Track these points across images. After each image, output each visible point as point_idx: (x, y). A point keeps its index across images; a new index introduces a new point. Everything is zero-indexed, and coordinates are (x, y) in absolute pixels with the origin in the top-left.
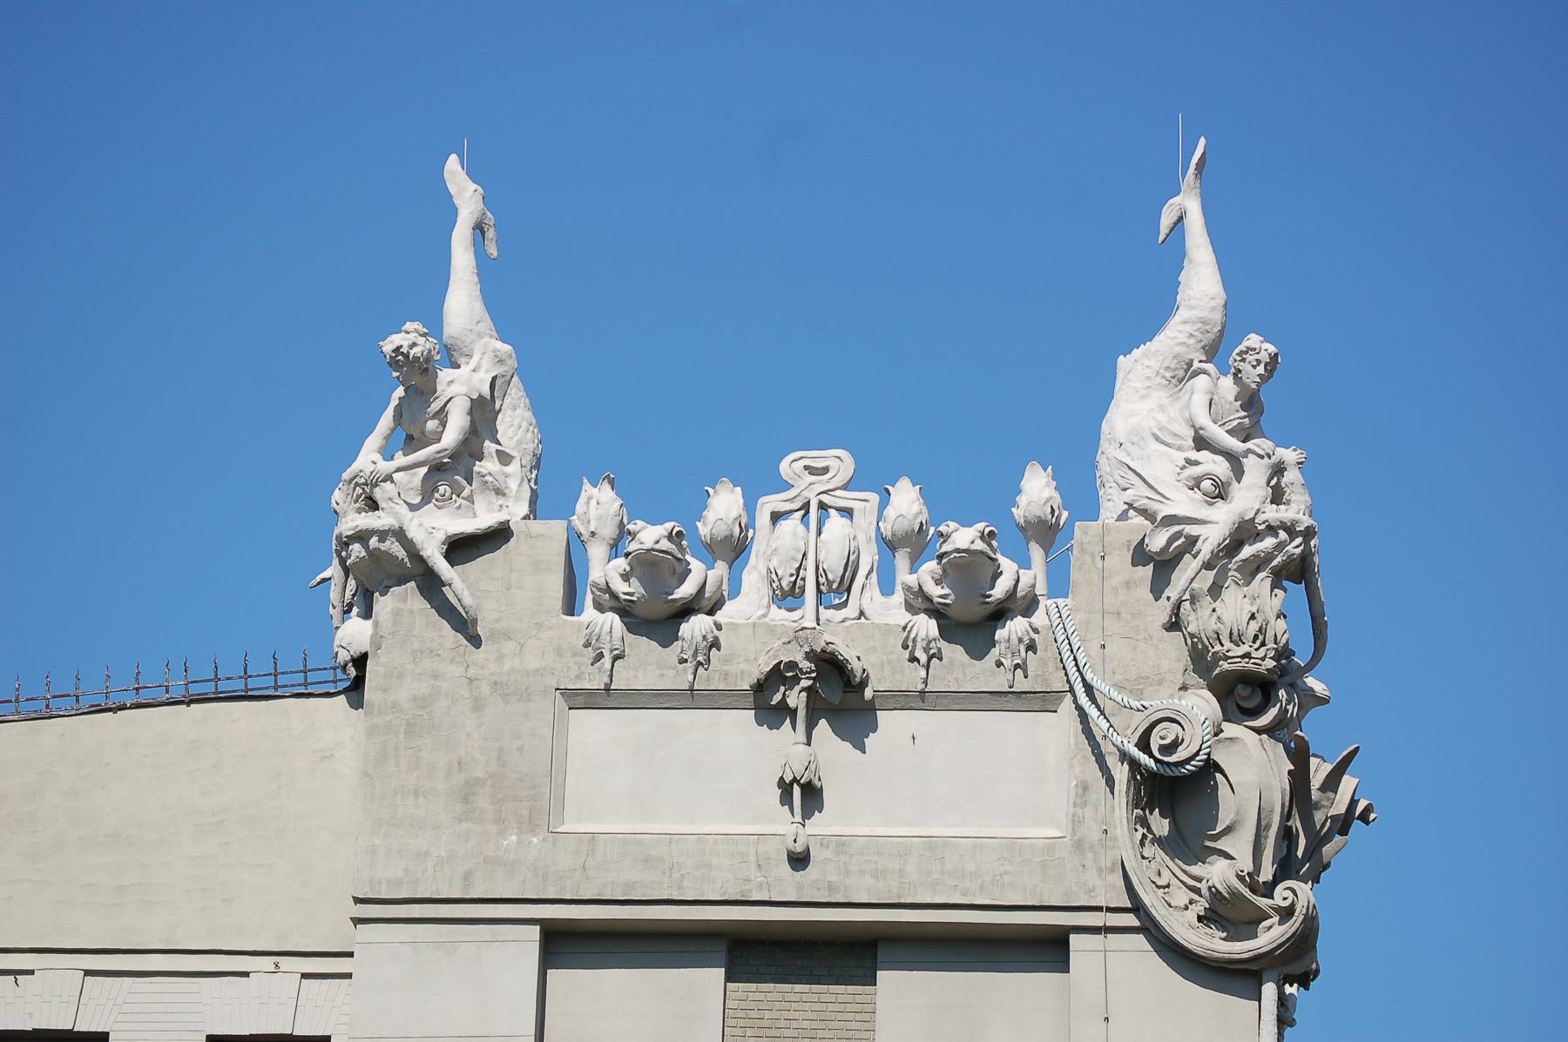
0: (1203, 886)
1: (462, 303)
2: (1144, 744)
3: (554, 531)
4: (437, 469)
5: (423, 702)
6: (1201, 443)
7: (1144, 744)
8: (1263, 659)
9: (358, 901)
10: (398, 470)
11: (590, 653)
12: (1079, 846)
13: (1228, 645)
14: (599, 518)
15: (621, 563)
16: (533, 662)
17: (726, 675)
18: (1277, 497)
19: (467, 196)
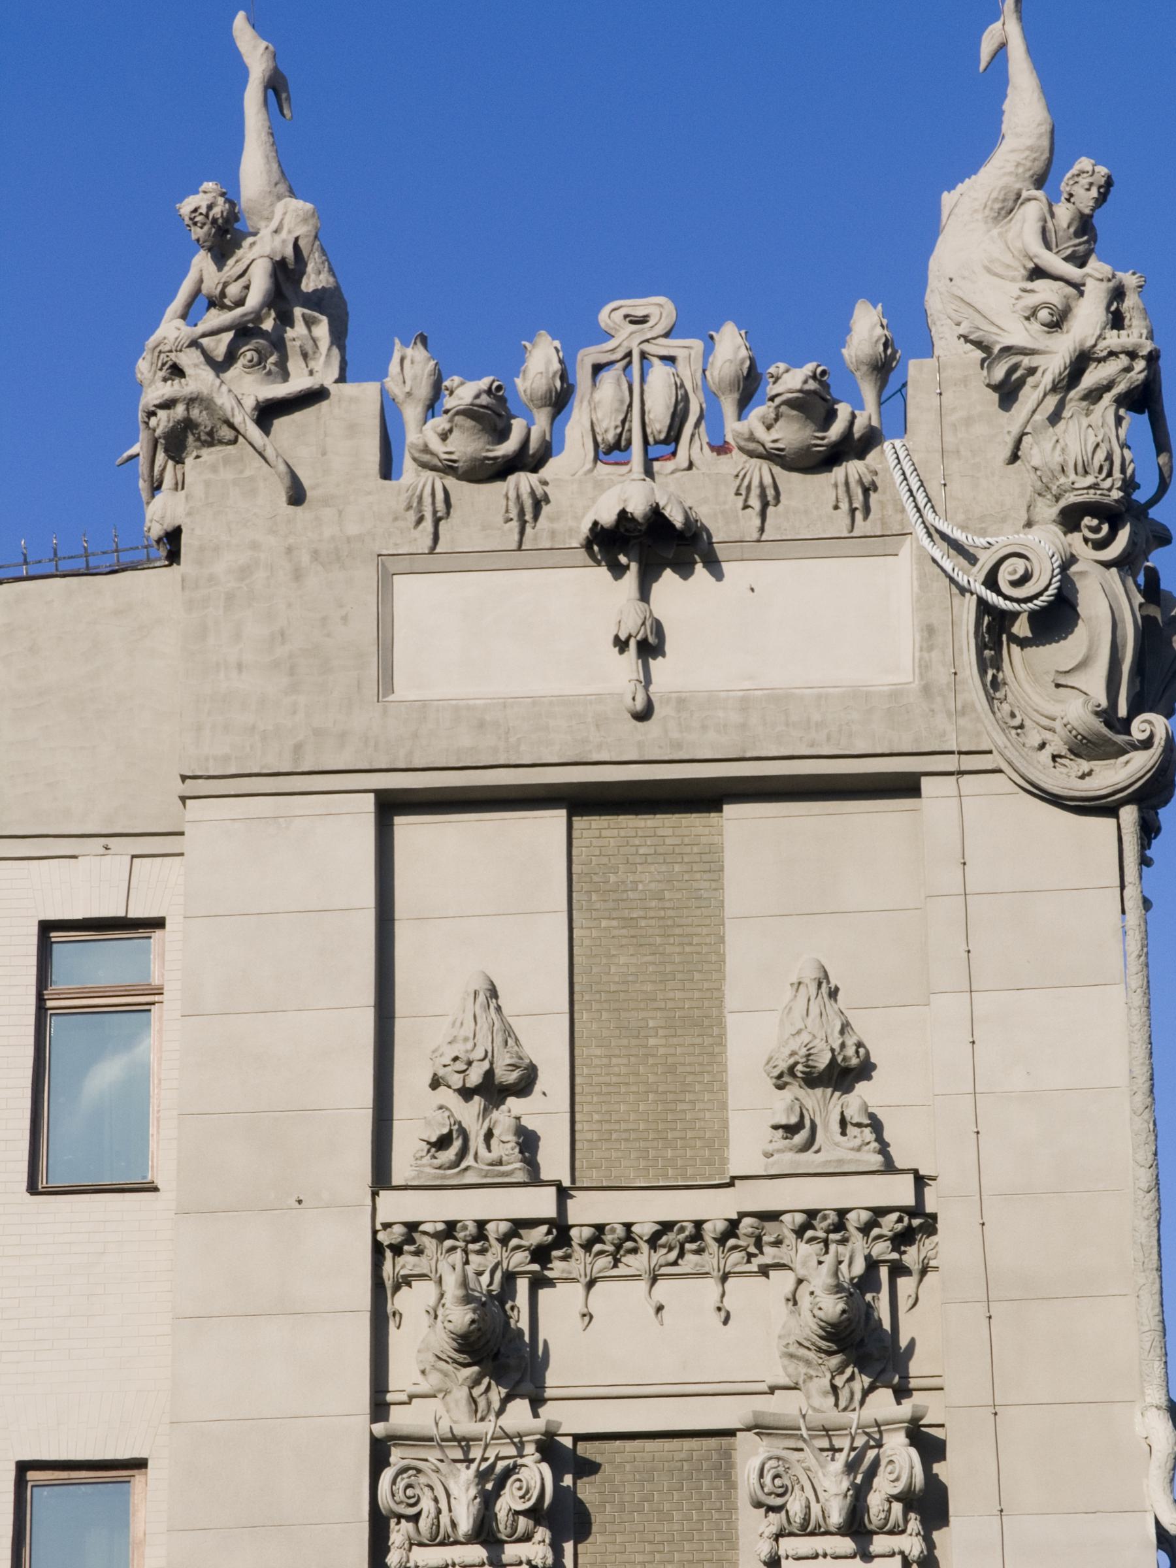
0: (1057, 725)
1: (255, 167)
2: (991, 582)
3: (370, 390)
4: (244, 332)
5: (244, 572)
6: (1038, 273)
7: (991, 582)
8: (1110, 490)
9: (184, 778)
10: (204, 335)
11: (412, 516)
12: (926, 690)
13: (1073, 477)
14: (415, 378)
15: (441, 422)
16: (352, 529)
17: (553, 534)
18: (1117, 321)
19: (255, 53)
